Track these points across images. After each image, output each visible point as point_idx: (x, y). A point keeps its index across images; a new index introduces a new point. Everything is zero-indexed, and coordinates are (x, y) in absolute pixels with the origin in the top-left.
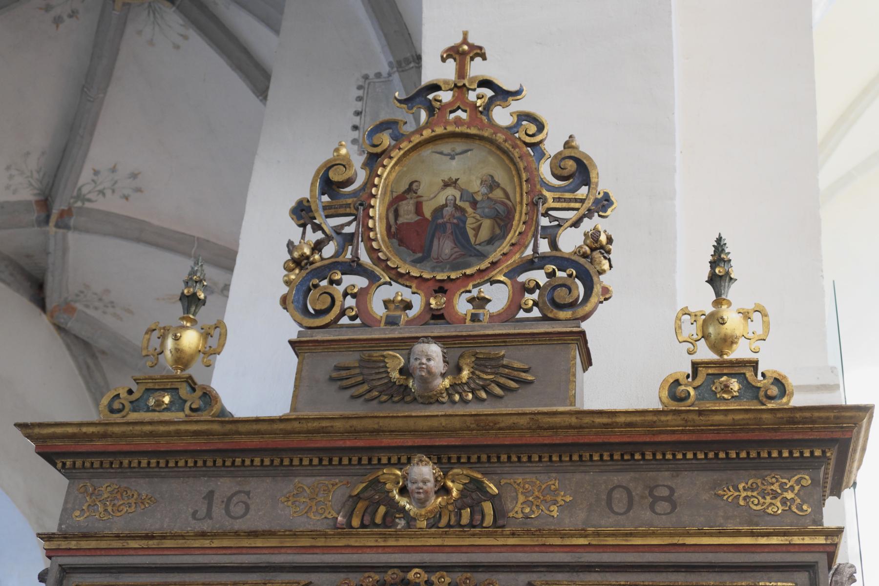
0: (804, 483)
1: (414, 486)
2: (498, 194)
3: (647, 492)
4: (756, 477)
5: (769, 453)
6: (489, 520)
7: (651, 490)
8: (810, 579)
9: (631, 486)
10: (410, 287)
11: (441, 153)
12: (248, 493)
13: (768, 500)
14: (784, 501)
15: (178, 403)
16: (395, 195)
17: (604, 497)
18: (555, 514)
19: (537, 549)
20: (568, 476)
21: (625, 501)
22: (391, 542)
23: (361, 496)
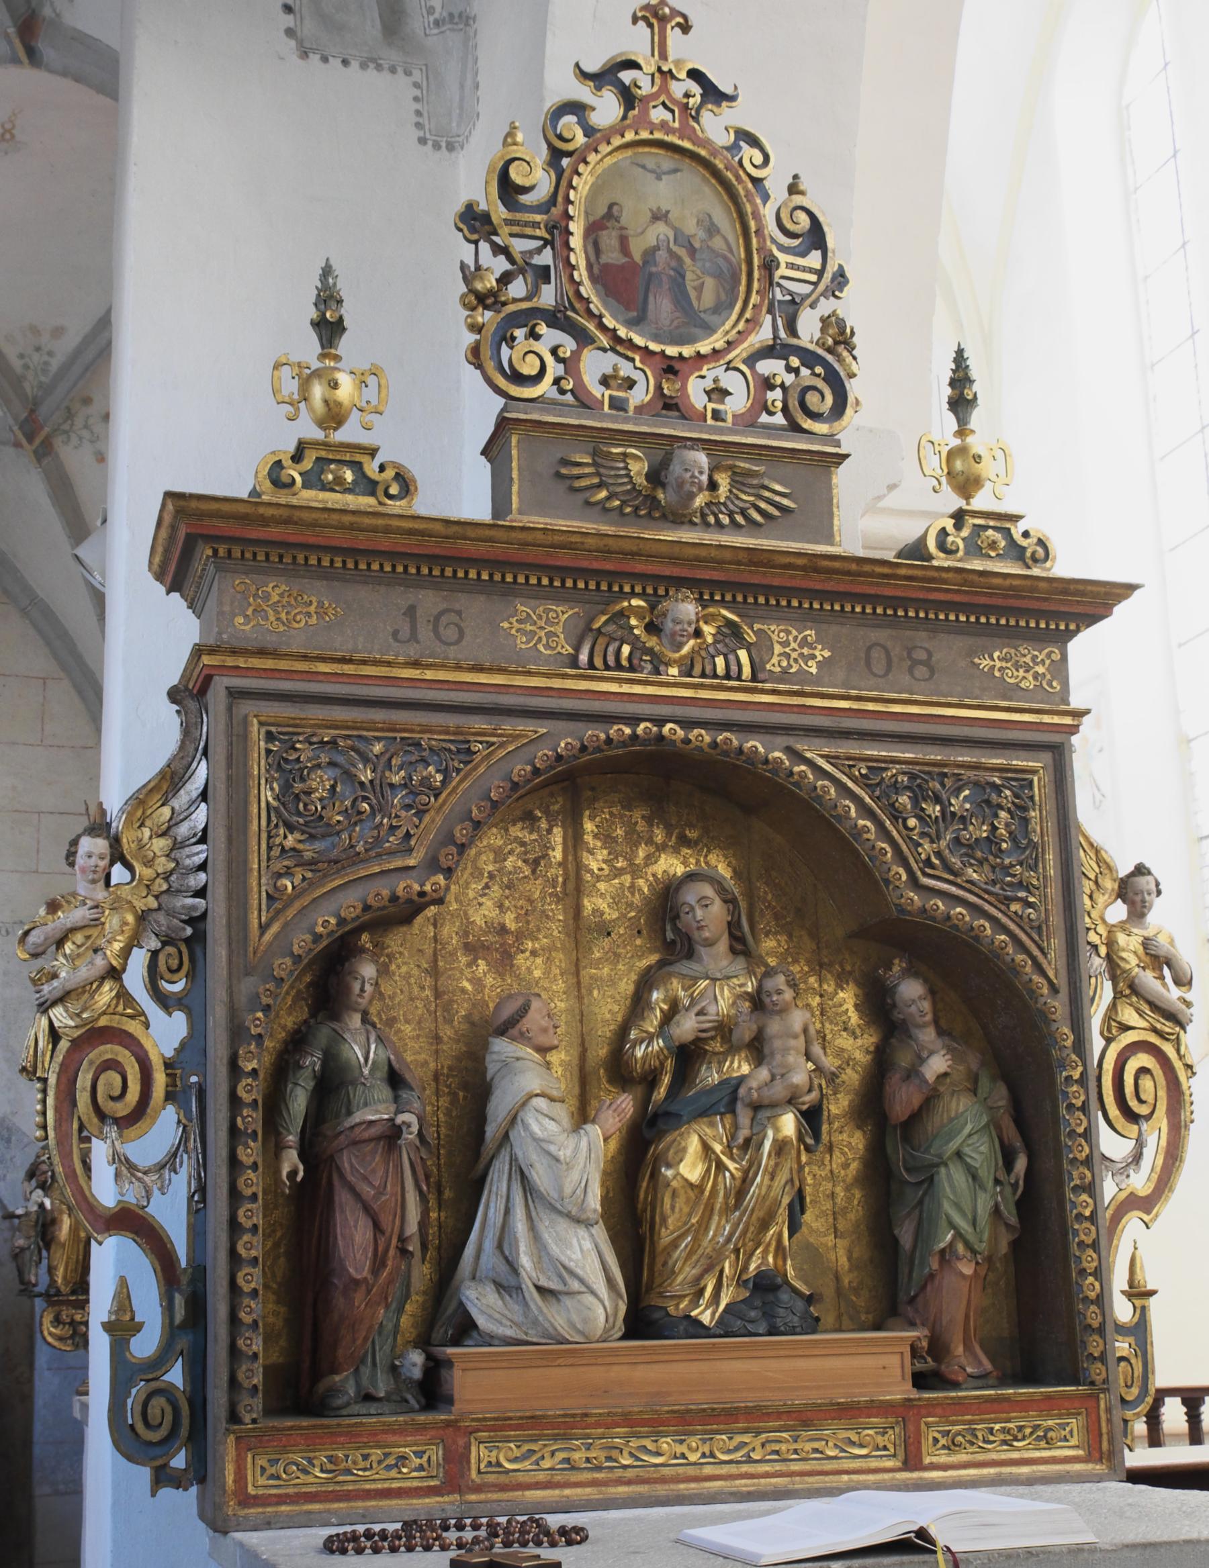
0: (1054, 657)
1: (678, 627)
2: (717, 243)
3: (905, 654)
4: (1008, 646)
5: (1027, 622)
6: (747, 671)
7: (910, 651)
8: (1054, 760)
9: (889, 644)
10: (632, 360)
11: (643, 167)
12: (459, 613)
13: (1021, 673)
14: (1036, 676)
15: (370, 486)
16: (591, 219)
17: (863, 655)
18: (814, 670)
19: (795, 709)
20: (824, 626)
21: (884, 662)
22: (638, 689)
23: (603, 630)
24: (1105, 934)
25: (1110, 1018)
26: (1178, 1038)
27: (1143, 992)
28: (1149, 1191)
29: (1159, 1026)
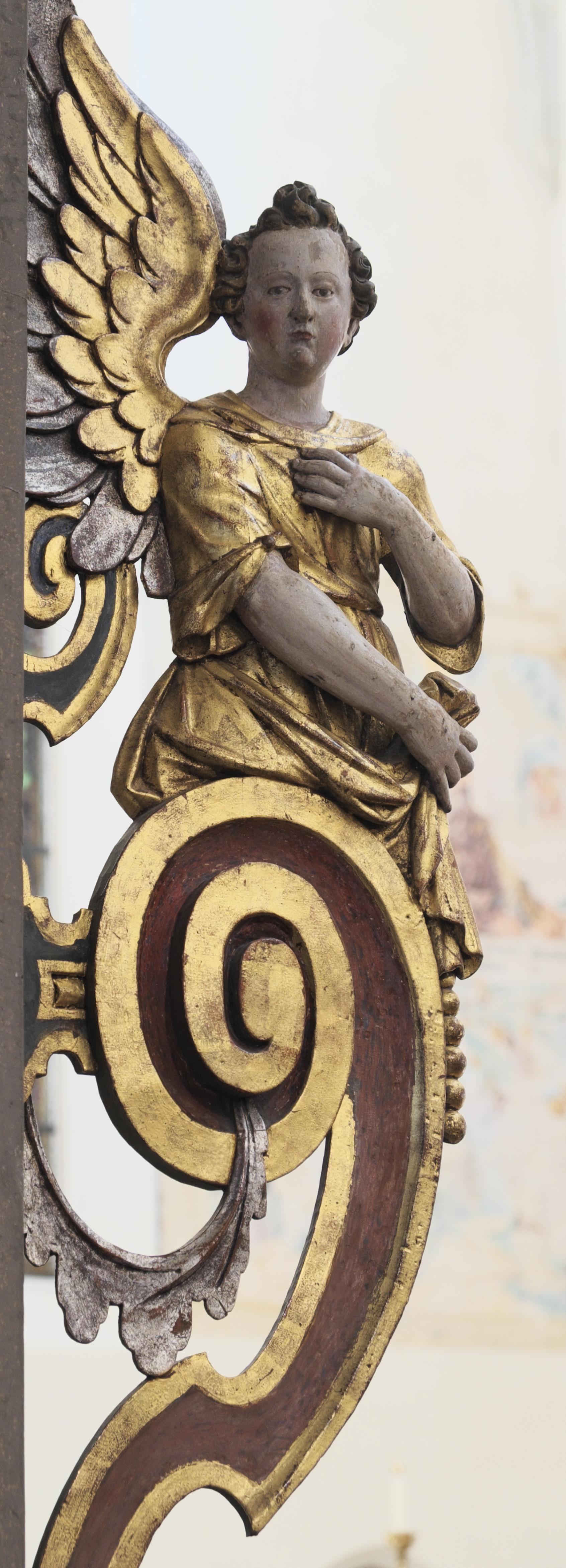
24: (153, 432)
25: (154, 732)
26: (412, 821)
27: (280, 642)
28: (267, 1388)
29: (335, 769)
